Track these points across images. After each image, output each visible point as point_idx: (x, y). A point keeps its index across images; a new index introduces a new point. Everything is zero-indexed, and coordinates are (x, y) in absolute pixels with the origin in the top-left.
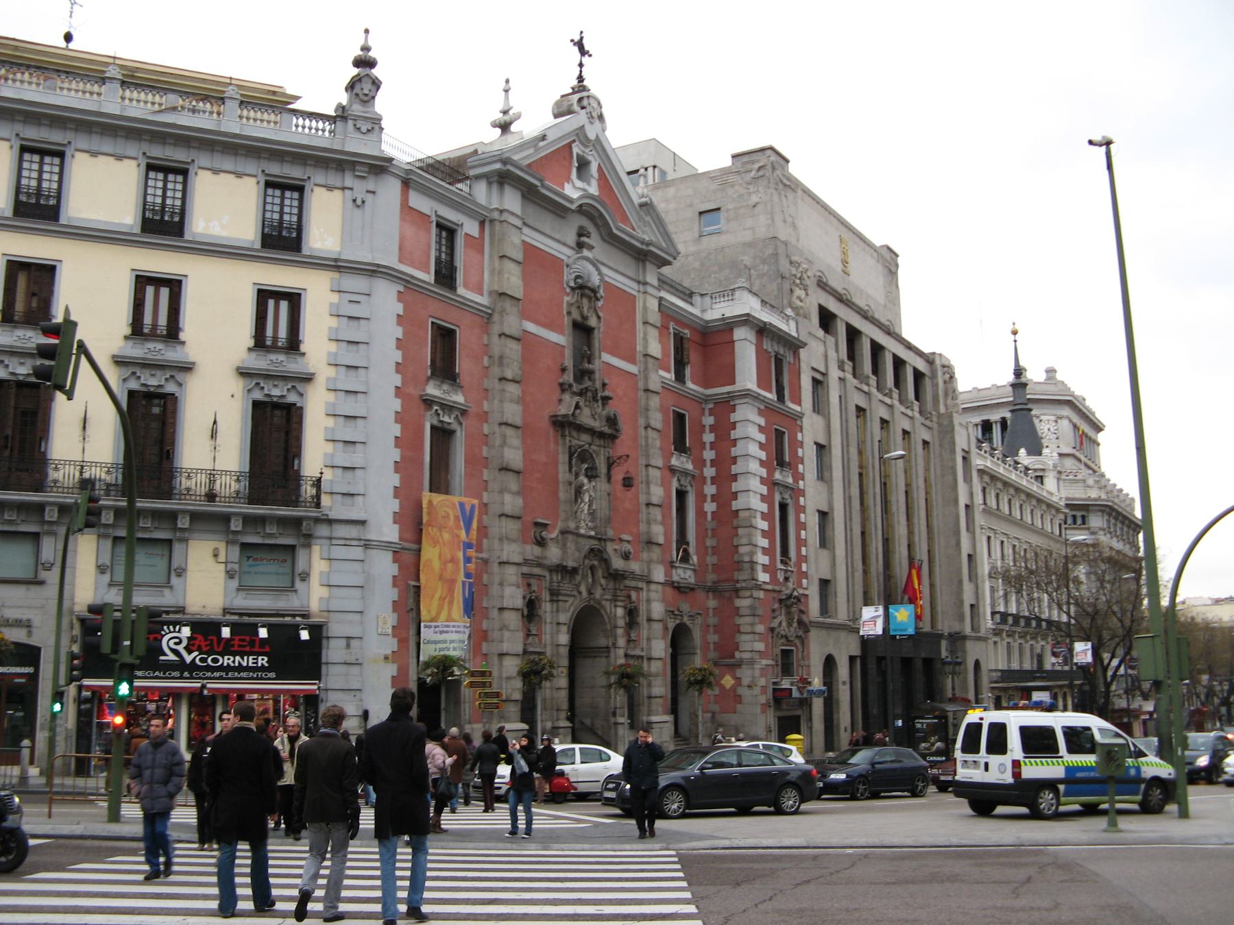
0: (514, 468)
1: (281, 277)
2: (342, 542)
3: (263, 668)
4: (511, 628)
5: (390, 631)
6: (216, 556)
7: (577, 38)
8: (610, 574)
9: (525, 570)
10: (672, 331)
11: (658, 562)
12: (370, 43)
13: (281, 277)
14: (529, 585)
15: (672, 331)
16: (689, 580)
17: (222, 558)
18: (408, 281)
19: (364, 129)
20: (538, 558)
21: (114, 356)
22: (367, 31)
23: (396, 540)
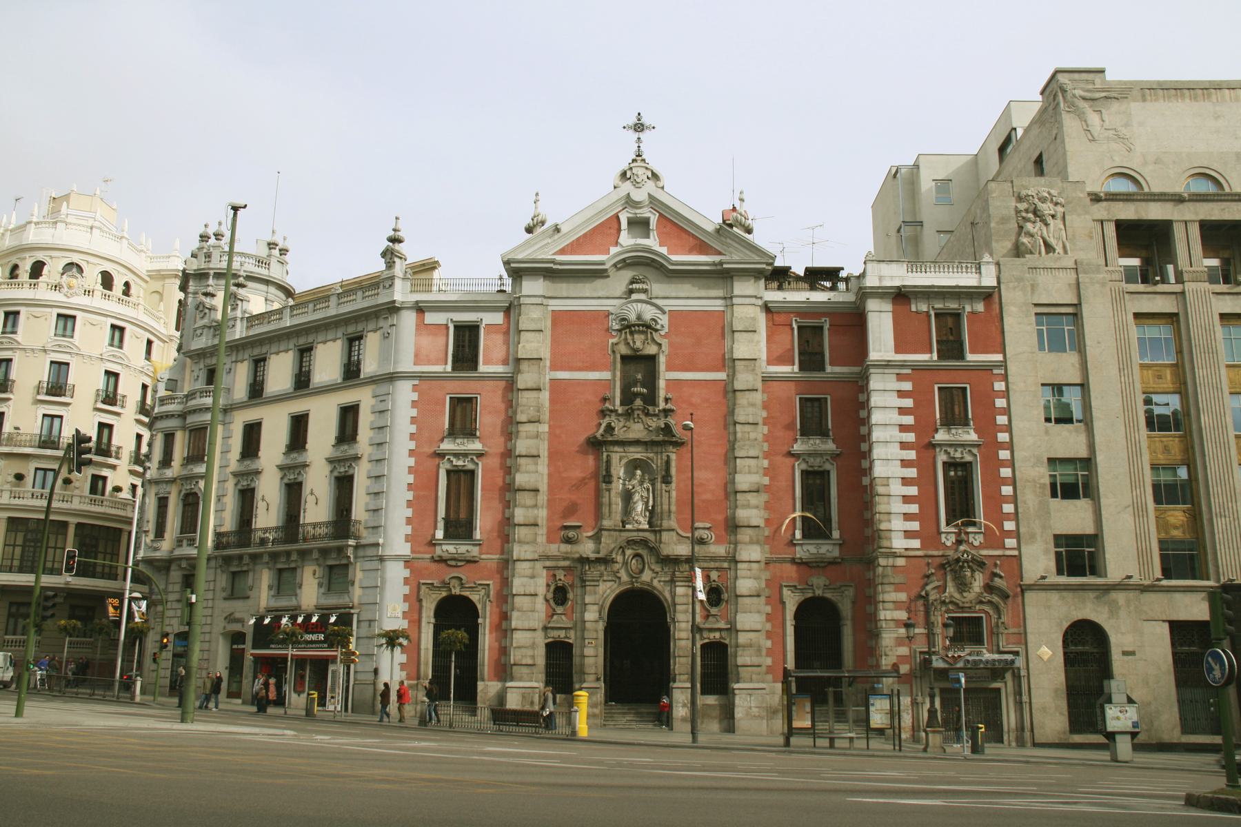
0: (527, 488)
1: (348, 397)
2: (369, 559)
3: (321, 642)
4: (524, 609)
5: (400, 615)
6: (314, 574)
7: (632, 120)
8: (662, 559)
9: (548, 564)
10: (795, 326)
11: (751, 542)
12: (400, 226)
13: (348, 397)
14: (555, 576)
15: (795, 326)
16: (829, 555)
17: (317, 576)
18: (420, 377)
19: (387, 286)
20: (567, 553)
21: (326, 459)
22: (397, 218)
23: (409, 554)
